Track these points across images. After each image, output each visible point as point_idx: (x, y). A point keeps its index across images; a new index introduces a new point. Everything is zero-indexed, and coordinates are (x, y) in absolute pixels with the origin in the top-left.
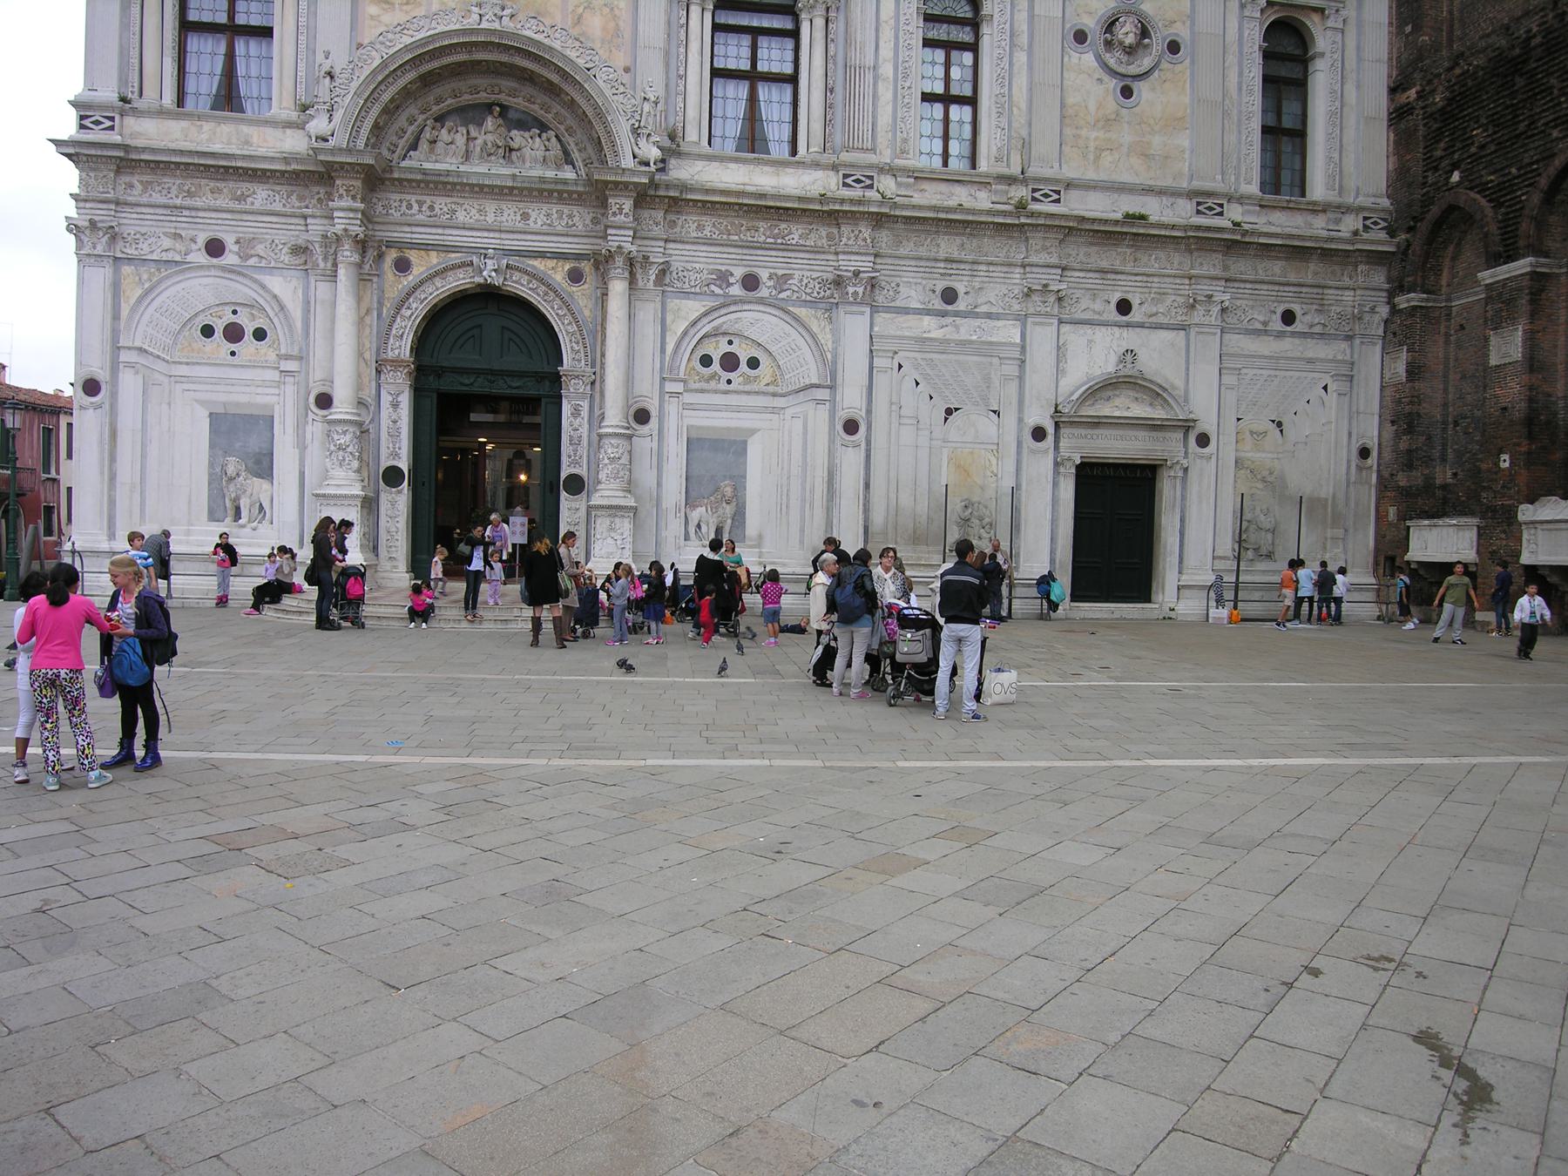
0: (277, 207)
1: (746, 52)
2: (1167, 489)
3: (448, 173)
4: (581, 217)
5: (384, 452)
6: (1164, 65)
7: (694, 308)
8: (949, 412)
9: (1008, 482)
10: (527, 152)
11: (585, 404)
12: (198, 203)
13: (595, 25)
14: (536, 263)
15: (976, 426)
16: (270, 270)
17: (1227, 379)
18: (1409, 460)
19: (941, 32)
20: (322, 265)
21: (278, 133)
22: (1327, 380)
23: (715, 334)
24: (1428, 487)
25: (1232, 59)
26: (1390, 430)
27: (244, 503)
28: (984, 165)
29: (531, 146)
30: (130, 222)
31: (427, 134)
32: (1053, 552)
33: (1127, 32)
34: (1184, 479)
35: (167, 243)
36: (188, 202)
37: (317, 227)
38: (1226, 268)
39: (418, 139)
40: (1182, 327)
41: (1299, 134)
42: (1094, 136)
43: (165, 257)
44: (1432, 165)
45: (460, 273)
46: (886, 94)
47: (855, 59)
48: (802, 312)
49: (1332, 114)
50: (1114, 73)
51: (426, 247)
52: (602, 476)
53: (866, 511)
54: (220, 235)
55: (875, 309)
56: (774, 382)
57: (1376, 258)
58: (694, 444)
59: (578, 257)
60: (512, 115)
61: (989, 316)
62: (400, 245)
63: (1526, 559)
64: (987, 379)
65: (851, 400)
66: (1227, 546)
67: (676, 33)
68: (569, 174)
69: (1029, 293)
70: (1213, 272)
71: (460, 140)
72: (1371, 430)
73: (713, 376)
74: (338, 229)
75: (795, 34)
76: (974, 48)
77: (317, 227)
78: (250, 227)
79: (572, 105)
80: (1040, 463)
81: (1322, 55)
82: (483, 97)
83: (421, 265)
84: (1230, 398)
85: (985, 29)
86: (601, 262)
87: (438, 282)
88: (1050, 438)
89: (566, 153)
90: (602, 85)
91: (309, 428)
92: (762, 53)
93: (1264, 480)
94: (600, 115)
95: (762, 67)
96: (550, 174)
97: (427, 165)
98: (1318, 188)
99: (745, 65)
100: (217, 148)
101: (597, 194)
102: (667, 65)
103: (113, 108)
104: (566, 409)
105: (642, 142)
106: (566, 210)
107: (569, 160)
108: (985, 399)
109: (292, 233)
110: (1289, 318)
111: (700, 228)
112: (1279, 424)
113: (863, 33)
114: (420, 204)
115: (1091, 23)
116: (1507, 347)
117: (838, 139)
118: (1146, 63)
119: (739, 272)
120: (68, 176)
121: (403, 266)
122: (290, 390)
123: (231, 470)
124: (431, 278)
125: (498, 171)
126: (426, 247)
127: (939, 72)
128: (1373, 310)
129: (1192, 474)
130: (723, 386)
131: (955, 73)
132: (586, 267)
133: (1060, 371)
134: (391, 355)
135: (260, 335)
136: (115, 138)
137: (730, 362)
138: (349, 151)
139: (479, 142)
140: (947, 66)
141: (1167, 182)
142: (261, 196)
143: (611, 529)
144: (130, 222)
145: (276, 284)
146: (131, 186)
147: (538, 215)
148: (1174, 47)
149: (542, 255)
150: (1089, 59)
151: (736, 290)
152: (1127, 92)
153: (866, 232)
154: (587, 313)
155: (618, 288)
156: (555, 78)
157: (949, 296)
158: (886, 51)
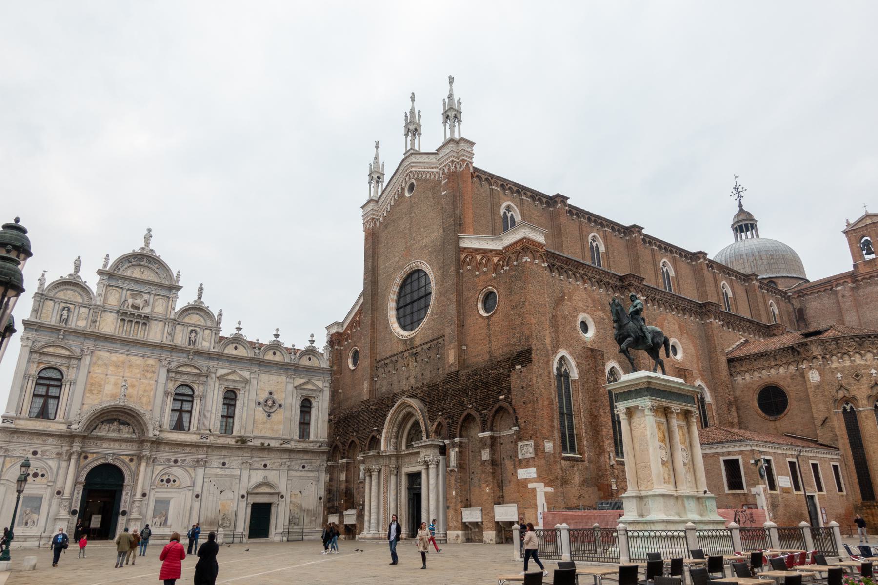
0: (54, 443)
1: (180, 405)
2: (273, 509)
3: (103, 436)
4: (135, 446)
5: (73, 506)
6: (278, 410)
7: (160, 468)
8: (222, 492)
9: (235, 509)
10: (124, 431)
11: (130, 492)
12: (33, 442)
13: (144, 400)
14: (122, 457)
15: (228, 495)
16: (49, 459)
17: (289, 482)
18: (329, 500)
19: (227, 401)
20: (65, 458)
21: (58, 425)
22: (312, 481)
23: (166, 474)
24: (333, 507)
25: (293, 408)
26: (326, 493)
27: (29, 521)
29: (125, 429)
30: (11, 447)
31: (99, 426)
32: (244, 526)
33: (270, 403)
34: (277, 506)
35: (21, 452)
36: (29, 442)
38: (290, 456)
39: (96, 427)
40: (279, 470)
41: (309, 424)
42: (261, 426)
43: (20, 455)
44: (334, 433)
45: (102, 460)
46: (213, 417)
47: (207, 409)
48: (187, 468)
49: (315, 420)
50: (266, 412)
51: (93, 453)
52: (134, 511)
53: (199, 517)
54: (37, 450)
55: (206, 467)
56: (179, 486)
57: (323, 453)
58: (157, 501)
59: (133, 455)
60: (121, 421)
61: (233, 468)
62: (86, 453)
63: (345, 523)
64: (231, 483)
65: (198, 490)
66: (287, 523)
67: (164, 402)
68: (134, 436)
70: (286, 457)
71: (107, 427)
72: (322, 493)
75: (192, 402)
76: (234, 405)
77: (65, 448)
78: (46, 448)
79: (138, 421)
80: (243, 504)
82: (115, 417)
83: (91, 457)
84: (289, 486)
85: (237, 402)
86: (140, 458)
87: (95, 462)
88: (246, 498)
89: (134, 431)
90: (147, 417)
91: (53, 500)
92: (184, 406)
93: (297, 506)
94: (145, 423)
95: (183, 409)
96: (130, 436)
97: (99, 434)
98: (312, 438)
99: (179, 408)
100: (41, 428)
101: (141, 442)
102: (161, 410)
103: (13, 418)
104: (124, 493)
105: (155, 431)
106: (131, 444)
107: (134, 432)
108: (231, 489)
109: (58, 449)
110: (304, 467)
113: (209, 403)
114: (94, 442)
115: (262, 400)
116: (343, 477)
117: (201, 427)
118: (274, 409)
119: (173, 459)
121: (86, 458)
122: (49, 490)
123: (28, 512)
124: (93, 461)
125: (117, 435)
126: (93, 453)
127: (226, 410)
128: (323, 465)
129: (280, 505)
130: (166, 487)
132: (135, 458)
133: (249, 481)
135: (43, 476)
136: (12, 425)
137: (168, 481)
138: (81, 432)
139: (112, 428)
140: (228, 409)
141: (276, 436)
142: (50, 440)
143: (135, 524)
144: (11, 447)
145: (50, 463)
146: (14, 437)
147: (124, 446)
148: (280, 406)
149: (123, 455)
150: (261, 408)
151: (172, 463)
152: (269, 416)
153: (205, 449)
154: (133, 469)
155: (143, 464)
156: (135, 415)
157: (224, 464)
158: (214, 407)
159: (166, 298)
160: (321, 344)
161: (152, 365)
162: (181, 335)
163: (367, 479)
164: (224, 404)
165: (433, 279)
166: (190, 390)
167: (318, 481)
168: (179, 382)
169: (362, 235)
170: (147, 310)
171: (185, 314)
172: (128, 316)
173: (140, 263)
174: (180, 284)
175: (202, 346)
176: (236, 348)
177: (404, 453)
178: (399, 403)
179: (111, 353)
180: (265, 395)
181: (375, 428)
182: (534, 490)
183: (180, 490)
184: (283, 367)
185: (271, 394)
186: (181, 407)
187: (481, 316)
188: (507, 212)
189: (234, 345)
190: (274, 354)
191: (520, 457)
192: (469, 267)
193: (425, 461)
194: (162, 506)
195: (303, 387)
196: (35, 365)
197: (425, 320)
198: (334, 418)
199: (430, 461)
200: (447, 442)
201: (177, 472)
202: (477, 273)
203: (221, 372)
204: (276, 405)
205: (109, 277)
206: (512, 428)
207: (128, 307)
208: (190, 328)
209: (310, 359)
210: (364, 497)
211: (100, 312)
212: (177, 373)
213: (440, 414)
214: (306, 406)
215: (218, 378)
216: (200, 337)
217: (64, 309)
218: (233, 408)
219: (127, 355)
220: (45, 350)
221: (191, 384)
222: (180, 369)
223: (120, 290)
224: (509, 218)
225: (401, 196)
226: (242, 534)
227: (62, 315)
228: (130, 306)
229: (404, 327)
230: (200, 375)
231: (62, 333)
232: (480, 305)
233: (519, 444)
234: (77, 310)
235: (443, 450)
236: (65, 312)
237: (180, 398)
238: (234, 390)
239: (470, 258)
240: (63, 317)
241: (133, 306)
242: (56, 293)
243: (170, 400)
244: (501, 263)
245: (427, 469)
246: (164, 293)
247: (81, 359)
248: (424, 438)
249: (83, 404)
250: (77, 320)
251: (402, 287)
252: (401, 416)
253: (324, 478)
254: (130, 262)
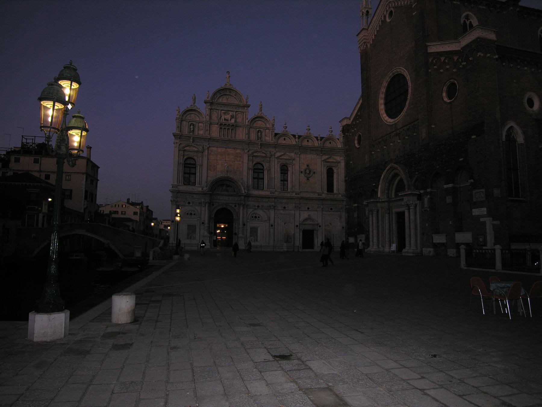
2: (315, 232)
6: (313, 175)
7: (251, 210)
8: (285, 223)
9: (293, 233)
28: (289, 190)
33: (308, 171)
37: (203, 200)
46: (276, 181)
54: (190, 201)
58: (251, 228)
65: (272, 222)
69: (295, 207)
72: (344, 224)
73: (254, 219)
74: (207, 201)
81: (335, 173)
85: (289, 172)
88: (299, 227)
95: (259, 177)
97: (217, 192)
98: (335, 191)
104: (234, 224)
110: (331, 209)
111: (252, 199)
112: (331, 224)
116: (356, 215)
119: (257, 205)
120: (170, 194)
121: (213, 205)
127: (283, 177)
131: (285, 177)
132: (237, 205)
133: (300, 218)
135: (194, 214)
137: (256, 217)
140: (284, 176)
142: (195, 196)
148: (314, 173)
150: (303, 175)
151: (256, 208)
158: (276, 175)
159: (242, 113)
160: (337, 133)
161: (239, 153)
162: (253, 134)
163: (370, 216)
164: (281, 173)
165: (409, 80)
166: (261, 166)
167: (341, 217)
168: (255, 162)
169: (358, 56)
170: (233, 121)
171: (253, 122)
173: (226, 93)
174: (248, 103)
175: (265, 140)
176: (285, 139)
177: (393, 200)
178: (389, 167)
179: (217, 148)
180: (305, 167)
181: (374, 184)
182: (484, 223)
183: (262, 222)
184: (313, 150)
185: (308, 166)
186: (258, 176)
187: (445, 102)
188: (466, 20)
189: (284, 137)
190: (308, 141)
191: (474, 200)
192: (435, 67)
193: (407, 205)
194: (254, 231)
195: (327, 160)
196: (182, 157)
197: (405, 109)
198: (348, 179)
199: (410, 204)
200: (422, 192)
201: (260, 212)
202: (441, 71)
203: (278, 154)
204: (312, 173)
205: (211, 104)
206: (469, 181)
207: (222, 120)
208: (257, 130)
209: (330, 143)
210: (369, 227)
211: (209, 125)
213: (417, 173)
214: (330, 173)
215: (276, 158)
216: (263, 134)
217: (191, 125)
218: (286, 175)
219: (226, 148)
220: (185, 148)
221: (262, 163)
222: (255, 154)
223: (217, 111)
224: (468, 25)
225: (384, 22)
226: (298, 247)
227: (190, 129)
228: (223, 120)
229: (390, 116)
230: (266, 157)
231: (192, 139)
232: (444, 94)
233: (474, 192)
234: (197, 124)
235: (420, 197)
236: (192, 127)
237: (257, 171)
238: (286, 165)
239: (436, 60)
240: (191, 130)
241: (225, 119)
242: (186, 116)
243: (251, 172)
244: (460, 60)
245: (409, 209)
246: (241, 110)
247: (203, 152)
248: (406, 190)
249: (208, 176)
250: (198, 130)
251: (388, 88)
252: (390, 176)
253: (344, 215)
254: (221, 94)
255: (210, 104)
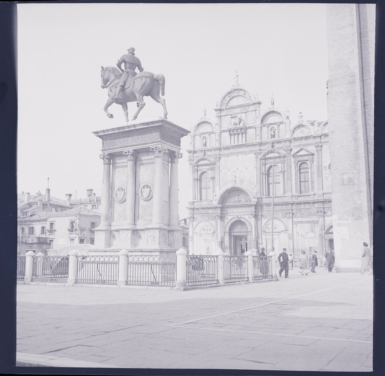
134: (226, 231)
172: (232, 132)
212: (266, 159)
222: (267, 156)
228: (233, 125)
255: (219, 112)
